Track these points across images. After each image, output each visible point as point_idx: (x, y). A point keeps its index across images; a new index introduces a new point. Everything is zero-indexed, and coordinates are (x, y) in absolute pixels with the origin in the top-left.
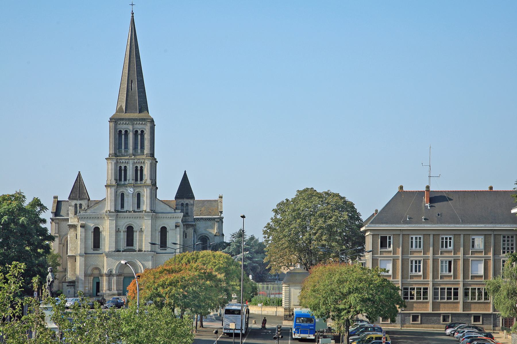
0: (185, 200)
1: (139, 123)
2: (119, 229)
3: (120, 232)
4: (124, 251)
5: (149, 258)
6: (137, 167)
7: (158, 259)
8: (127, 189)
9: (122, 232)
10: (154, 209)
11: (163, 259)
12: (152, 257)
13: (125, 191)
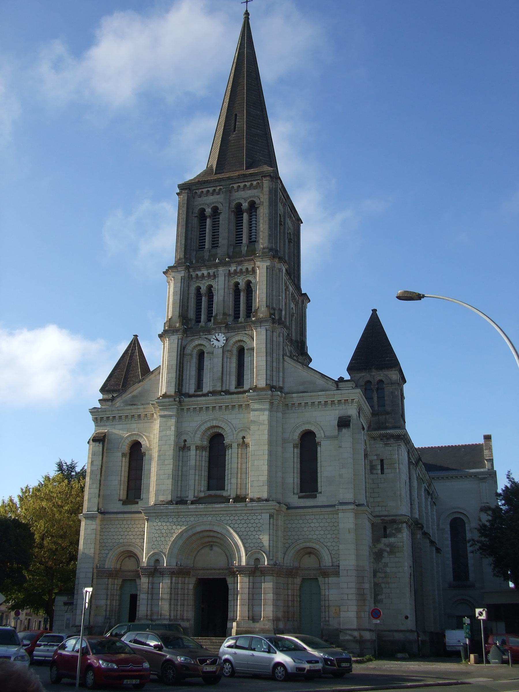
0: (374, 373)
1: (245, 185)
2: (185, 441)
3: (189, 449)
4: (197, 501)
5: (261, 521)
6: (237, 284)
7: (294, 526)
8: (209, 337)
9: (193, 448)
10: (281, 385)
11: (308, 525)
12: (271, 516)
13: (204, 343)
